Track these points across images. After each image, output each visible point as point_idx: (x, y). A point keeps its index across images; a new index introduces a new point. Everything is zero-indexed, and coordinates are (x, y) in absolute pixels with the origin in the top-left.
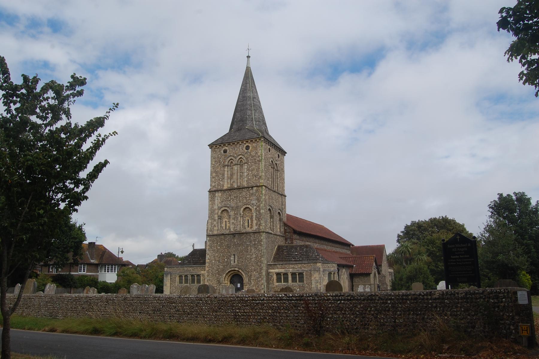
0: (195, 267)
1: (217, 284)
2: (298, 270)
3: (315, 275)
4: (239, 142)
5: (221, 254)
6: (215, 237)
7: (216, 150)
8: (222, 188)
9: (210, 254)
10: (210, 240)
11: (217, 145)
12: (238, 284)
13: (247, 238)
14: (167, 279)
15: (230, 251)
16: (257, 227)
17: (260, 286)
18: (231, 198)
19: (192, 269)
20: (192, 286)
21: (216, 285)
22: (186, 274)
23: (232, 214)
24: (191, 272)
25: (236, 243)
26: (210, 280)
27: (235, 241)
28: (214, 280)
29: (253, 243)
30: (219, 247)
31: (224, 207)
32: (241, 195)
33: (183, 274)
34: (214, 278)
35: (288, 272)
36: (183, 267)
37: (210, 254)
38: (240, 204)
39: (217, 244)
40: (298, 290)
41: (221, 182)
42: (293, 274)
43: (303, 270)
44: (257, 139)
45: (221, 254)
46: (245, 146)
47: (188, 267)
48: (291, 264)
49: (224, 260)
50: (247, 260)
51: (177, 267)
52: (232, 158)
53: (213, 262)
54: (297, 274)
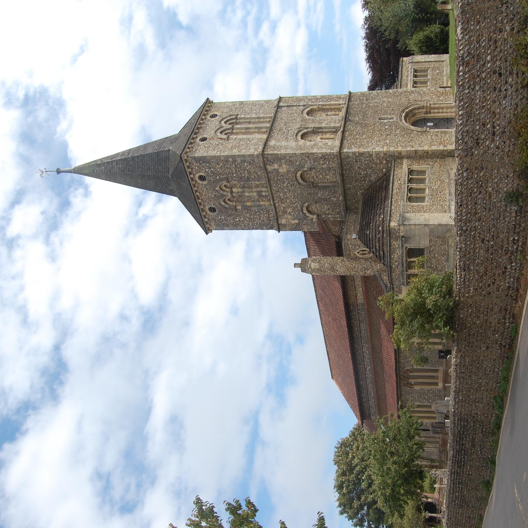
0: (393, 177)
1: (426, 135)
2: (411, 72)
3: (418, 59)
4: (198, 122)
5: (375, 134)
6: (345, 142)
7: (194, 150)
8: (262, 140)
9: (373, 146)
10: (348, 148)
11: (187, 146)
12: (428, 125)
13: (355, 108)
14: (414, 218)
15: (373, 123)
16: (342, 101)
17: (432, 92)
18: (286, 129)
19: (397, 182)
20: (429, 180)
21: (429, 137)
22: (406, 189)
23: (312, 126)
24: (402, 183)
25: (360, 117)
26: (420, 144)
27: (357, 119)
28: (420, 139)
29: (365, 101)
30: (362, 136)
31: (296, 136)
32: (285, 119)
33: (406, 193)
34: (417, 139)
35: (412, 80)
36: (392, 194)
37: (373, 146)
38: (299, 119)
39: (357, 138)
40: (438, 71)
41: (253, 142)
42: (415, 76)
43: (411, 69)
44: (206, 104)
45: (375, 134)
46: (210, 118)
47: (392, 187)
48: (401, 78)
49: (386, 129)
50: (391, 105)
51: (391, 205)
52: (220, 131)
53: (388, 141)
54: (415, 74)
